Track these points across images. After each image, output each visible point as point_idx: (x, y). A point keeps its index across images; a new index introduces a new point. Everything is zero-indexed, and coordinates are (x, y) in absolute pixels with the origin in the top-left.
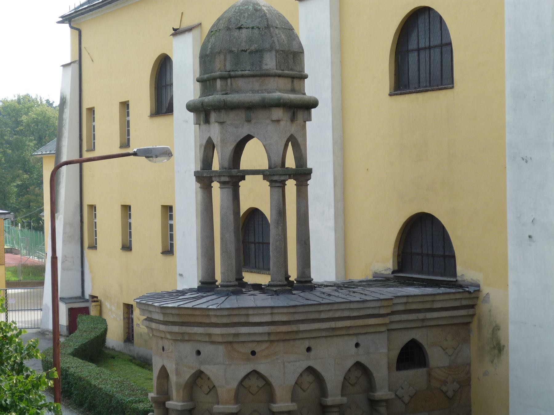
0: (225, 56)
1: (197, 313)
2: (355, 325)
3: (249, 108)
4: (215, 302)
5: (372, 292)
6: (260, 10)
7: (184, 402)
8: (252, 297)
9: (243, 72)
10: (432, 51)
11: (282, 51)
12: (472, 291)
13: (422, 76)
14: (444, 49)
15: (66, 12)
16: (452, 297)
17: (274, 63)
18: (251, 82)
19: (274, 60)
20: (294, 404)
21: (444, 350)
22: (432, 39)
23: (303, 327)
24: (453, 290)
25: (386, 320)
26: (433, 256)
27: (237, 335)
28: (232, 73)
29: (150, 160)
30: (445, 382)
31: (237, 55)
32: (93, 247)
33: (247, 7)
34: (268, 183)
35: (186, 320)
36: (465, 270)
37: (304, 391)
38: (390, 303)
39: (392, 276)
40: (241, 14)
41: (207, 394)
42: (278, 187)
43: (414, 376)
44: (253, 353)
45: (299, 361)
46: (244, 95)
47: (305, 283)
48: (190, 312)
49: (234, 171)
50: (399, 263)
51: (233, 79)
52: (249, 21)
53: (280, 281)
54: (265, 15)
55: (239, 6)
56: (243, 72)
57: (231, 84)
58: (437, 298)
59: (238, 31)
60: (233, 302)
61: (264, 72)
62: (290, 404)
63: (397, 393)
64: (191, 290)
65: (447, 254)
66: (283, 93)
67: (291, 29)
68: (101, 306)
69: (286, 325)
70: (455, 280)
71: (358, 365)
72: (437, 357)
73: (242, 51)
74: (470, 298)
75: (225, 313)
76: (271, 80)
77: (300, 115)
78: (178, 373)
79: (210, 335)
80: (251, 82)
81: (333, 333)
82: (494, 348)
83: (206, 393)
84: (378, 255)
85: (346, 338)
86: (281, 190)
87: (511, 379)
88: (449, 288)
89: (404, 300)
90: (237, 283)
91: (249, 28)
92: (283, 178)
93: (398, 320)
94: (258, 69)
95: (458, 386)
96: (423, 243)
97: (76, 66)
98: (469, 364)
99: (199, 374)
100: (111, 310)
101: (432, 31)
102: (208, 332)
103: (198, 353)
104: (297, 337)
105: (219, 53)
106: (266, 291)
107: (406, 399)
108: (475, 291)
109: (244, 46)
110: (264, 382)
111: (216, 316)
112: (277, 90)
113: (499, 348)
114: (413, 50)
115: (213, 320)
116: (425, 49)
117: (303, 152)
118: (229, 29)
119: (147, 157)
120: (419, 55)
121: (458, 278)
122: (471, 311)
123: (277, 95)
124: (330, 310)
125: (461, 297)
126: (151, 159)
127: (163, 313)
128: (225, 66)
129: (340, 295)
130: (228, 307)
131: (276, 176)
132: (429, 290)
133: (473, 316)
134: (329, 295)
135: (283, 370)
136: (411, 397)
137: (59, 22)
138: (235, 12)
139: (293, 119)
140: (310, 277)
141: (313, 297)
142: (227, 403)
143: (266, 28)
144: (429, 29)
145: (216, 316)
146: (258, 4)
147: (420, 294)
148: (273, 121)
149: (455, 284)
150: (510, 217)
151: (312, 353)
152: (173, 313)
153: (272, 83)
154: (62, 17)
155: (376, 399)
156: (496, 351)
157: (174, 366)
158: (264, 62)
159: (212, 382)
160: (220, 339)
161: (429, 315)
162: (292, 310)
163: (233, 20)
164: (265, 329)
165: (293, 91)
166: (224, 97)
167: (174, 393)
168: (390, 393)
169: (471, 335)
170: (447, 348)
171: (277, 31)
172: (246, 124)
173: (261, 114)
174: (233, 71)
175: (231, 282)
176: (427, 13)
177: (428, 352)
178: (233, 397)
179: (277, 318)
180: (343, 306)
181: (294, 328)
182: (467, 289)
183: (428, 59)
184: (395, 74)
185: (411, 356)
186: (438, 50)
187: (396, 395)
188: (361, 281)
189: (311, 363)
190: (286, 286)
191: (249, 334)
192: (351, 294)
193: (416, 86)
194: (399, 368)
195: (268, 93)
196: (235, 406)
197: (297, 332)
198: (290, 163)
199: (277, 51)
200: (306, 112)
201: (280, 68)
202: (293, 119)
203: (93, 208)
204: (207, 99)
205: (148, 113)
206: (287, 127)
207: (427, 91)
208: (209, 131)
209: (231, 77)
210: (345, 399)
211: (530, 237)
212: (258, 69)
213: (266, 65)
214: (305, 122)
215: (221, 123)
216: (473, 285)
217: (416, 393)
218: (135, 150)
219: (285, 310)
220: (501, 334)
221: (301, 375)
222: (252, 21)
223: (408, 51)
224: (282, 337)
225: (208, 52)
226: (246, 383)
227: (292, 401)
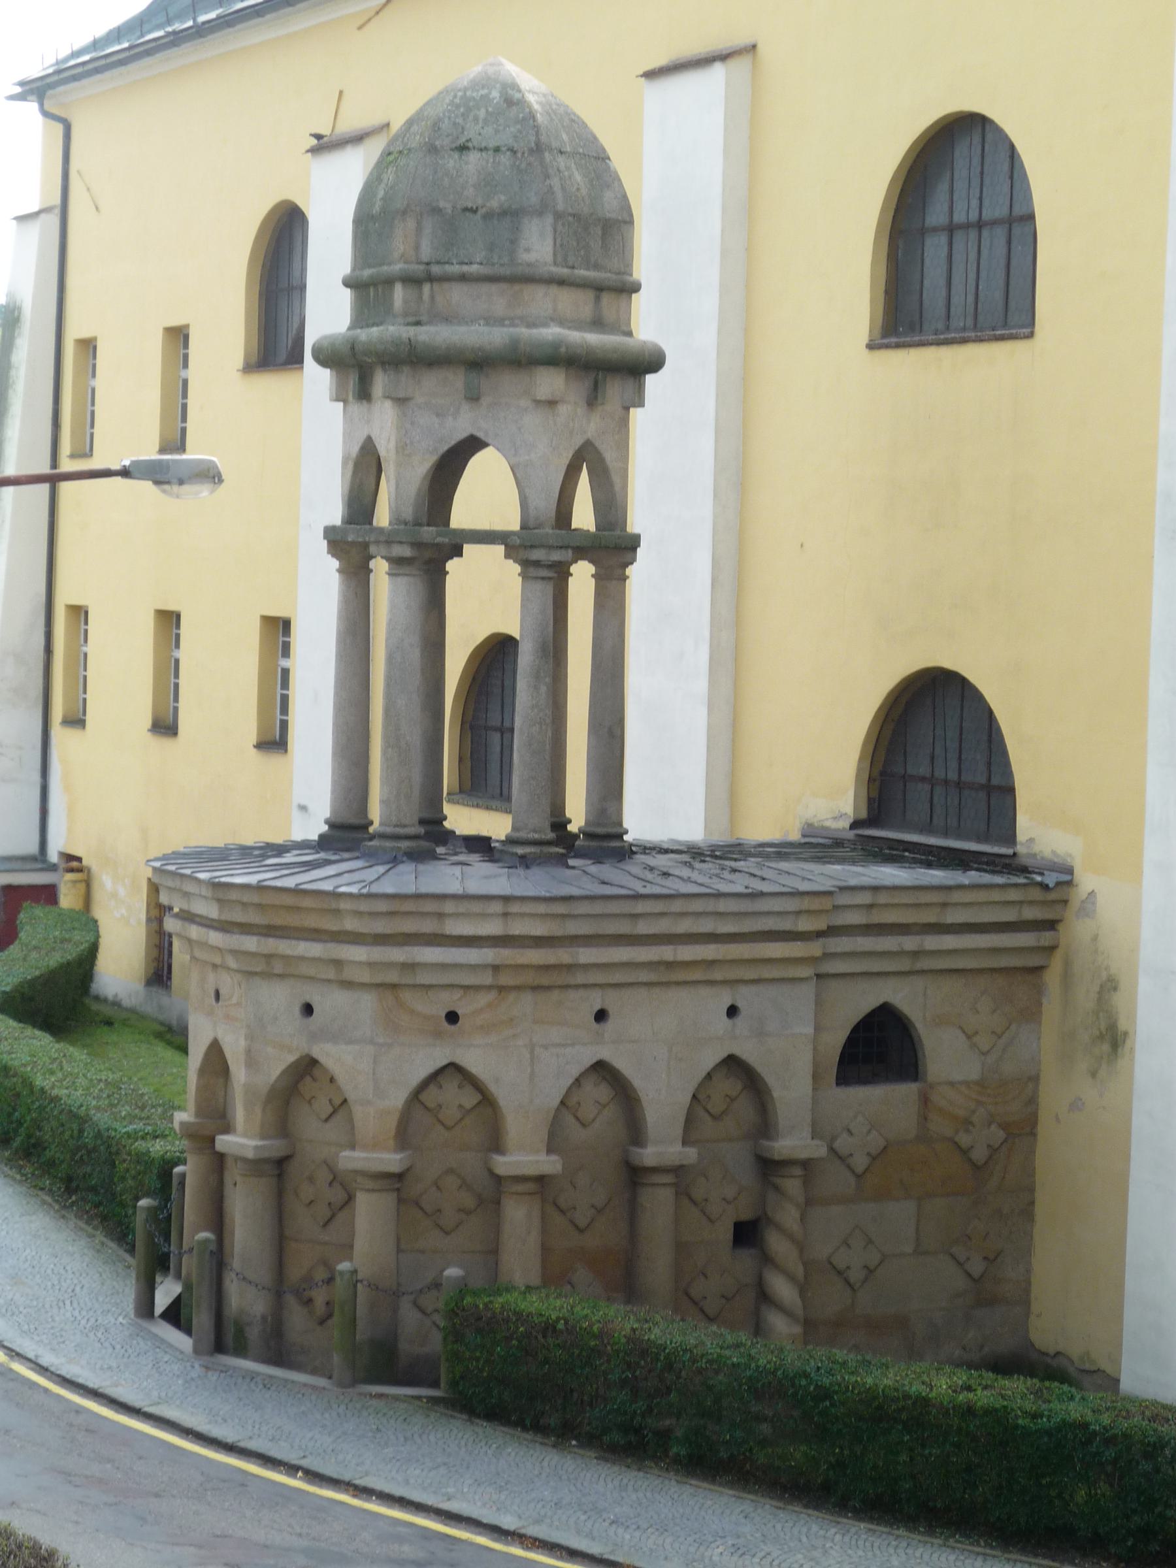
1: (307, 903)
2: (729, 957)
3: (478, 363)
4: (356, 876)
5: (781, 872)
6: (521, 103)
7: (263, 1138)
8: (457, 870)
9: (465, 268)
10: (985, 233)
11: (574, 216)
12: (1051, 885)
13: (956, 300)
14: (1017, 230)
15: (35, 70)
16: (996, 896)
18: (484, 295)
19: (549, 241)
20: (554, 1158)
21: (969, 1037)
22: (986, 203)
23: (586, 955)
24: (999, 880)
25: (814, 949)
26: (960, 785)
27: (410, 967)
28: (436, 270)
29: (164, 491)
30: (967, 1123)
31: (452, 221)
32: (76, 721)
33: (486, 91)
34: (517, 568)
35: (278, 921)
36: (1038, 830)
37: (584, 1125)
38: (827, 903)
39: (851, 835)
41: (326, 1120)
42: (543, 578)
43: (883, 1103)
44: (452, 1017)
45: (573, 1045)
47: (606, 841)
48: (289, 900)
49: (428, 533)
50: (870, 800)
51: (436, 286)
52: (489, 130)
53: (535, 831)
54: (532, 116)
55: (465, 90)
56: (465, 268)
57: (432, 297)
58: (957, 897)
59: (456, 155)
60: (405, 879)
62: (543, 1157)
63: (836, 1145)
64: (304, 845)
65: (995, 781)
66: (569, 328)
67: (602, 157)
68: (88, 884)
70: (1010, 851)
71: (732, 1063)
72: (947, 1055)
73: (466, 209)
74: (1044, 903)
75: (382, 906)
77: (615, 389)
78: (251, 1061)
79: (338, 963)
80: (484, 295)
81: (669, 977)
82: (1101, 1037)
83: (324, 1117)
84: (815, 777)
85: (704, 991)
86: (549, 588)
87: (1139, 1122)
88: (993, 872)
89: (864, 898)
90: (421, 830)
91: (486, 149)
92: (556, 556)
94: (506, 260)
95: (1002, 1134)
96: (935, 751)
97: (54, 220)
98: (1035, 1079)
99: (307, 1067)
100: (114, 895)
101: (987, 181)
102: (334, 956)
103: (308, 1009)
104: (571, 980)
105: (404, 212)
106: (497, 856)
107: (860, 1162)
108: (1058, 884)
109: (471, 197)
110: (479, 1097)
111: (359, 914)
112: (555, 321)
113: (1113, 1040)
114: (935, 230)
115: (350, 924)
116: (967, 226)
117: (617, 488)
118: (432, 149)
119: (157, 483)
120: (950, 244)
121: (1020, 849)
122: (1046, 938)
123: (551, 332)
124: (663, 914)
125: (1022, 899)
126: (166, 487)
127: (219, 901)
128: (417, 248)
129: (695, 876)
130: (390, 890)
131: (543, 549)
132: (937, 876)
133: (1052, 949)
134: (666, 874)
135: (528, 1066)
136: (874, 1159)
137: (12, 98)
138: (452, 103)
139: (593, 400)
140: (620, 824)
141: (622, 878)
142: (375, 1146)
143: (531, 151)
144: (982, 173)
145: (359, 914)
146: (515, 87)
147: (909, 883)
148: (538, 402)
149: (1010, 865)
151: (610, 1026)
152: (245, 900)
153: (541, 300)
154: (22, 84)
155: (776, 1157)
156: (1106, 1047)
157: (243, 1042)
159: (339, 1088)
160: (365, 977)
161: (932, 942)
162: (560, 909)
163: (445, 125)
164: (487, 955)
165: (598, 324)
167: (239, 1115)
168: (816, 1142)
169: (1044, 1001)
170: (976, 1033)
171: (561, 161)
172: (465, 407)
173: (508, 382)
174: (438, 263)
175: (405, 826)
177: (925, 1041)
178: (393, 1133)
179: (518, 928)
180: (698, 906)
181: (563, 956)
182: (1039, 878)
183: (973, 256)
184: (886, 292)
185: (879, 1048)
186: (1000, 233)
187: (832, 1150)
188: (762, 845)
189: (604, 1053)
190: (557, 843)
191: (444, 967)
192: (726, 875)
193: (941, 326)
194: (843, 1079)
195: (530, 325)
196: (398, 1156)
197: (570, 968)
198: (584, 517)
199: (558, 216)
200: (630, 383)
201: (565, 259)
202: (593, 400)
203: (79, 613)
205: (239, 361)
206: (577, 422)
207: (964, 341)
209: (431, 279)
210: (691, 1155)
212: (506, 260)
213: (528, 250)
214: (627, 409)
215: (401, 402)
217: (885, 1148)
218: (127, 463)
219: (542, 908)
220: (1119, 1000)
221: (577, 1082)
223: (923, 232)
224: (529, 978)
225: (377, 209)
226: (431, 1096)
227: (549, 1151)
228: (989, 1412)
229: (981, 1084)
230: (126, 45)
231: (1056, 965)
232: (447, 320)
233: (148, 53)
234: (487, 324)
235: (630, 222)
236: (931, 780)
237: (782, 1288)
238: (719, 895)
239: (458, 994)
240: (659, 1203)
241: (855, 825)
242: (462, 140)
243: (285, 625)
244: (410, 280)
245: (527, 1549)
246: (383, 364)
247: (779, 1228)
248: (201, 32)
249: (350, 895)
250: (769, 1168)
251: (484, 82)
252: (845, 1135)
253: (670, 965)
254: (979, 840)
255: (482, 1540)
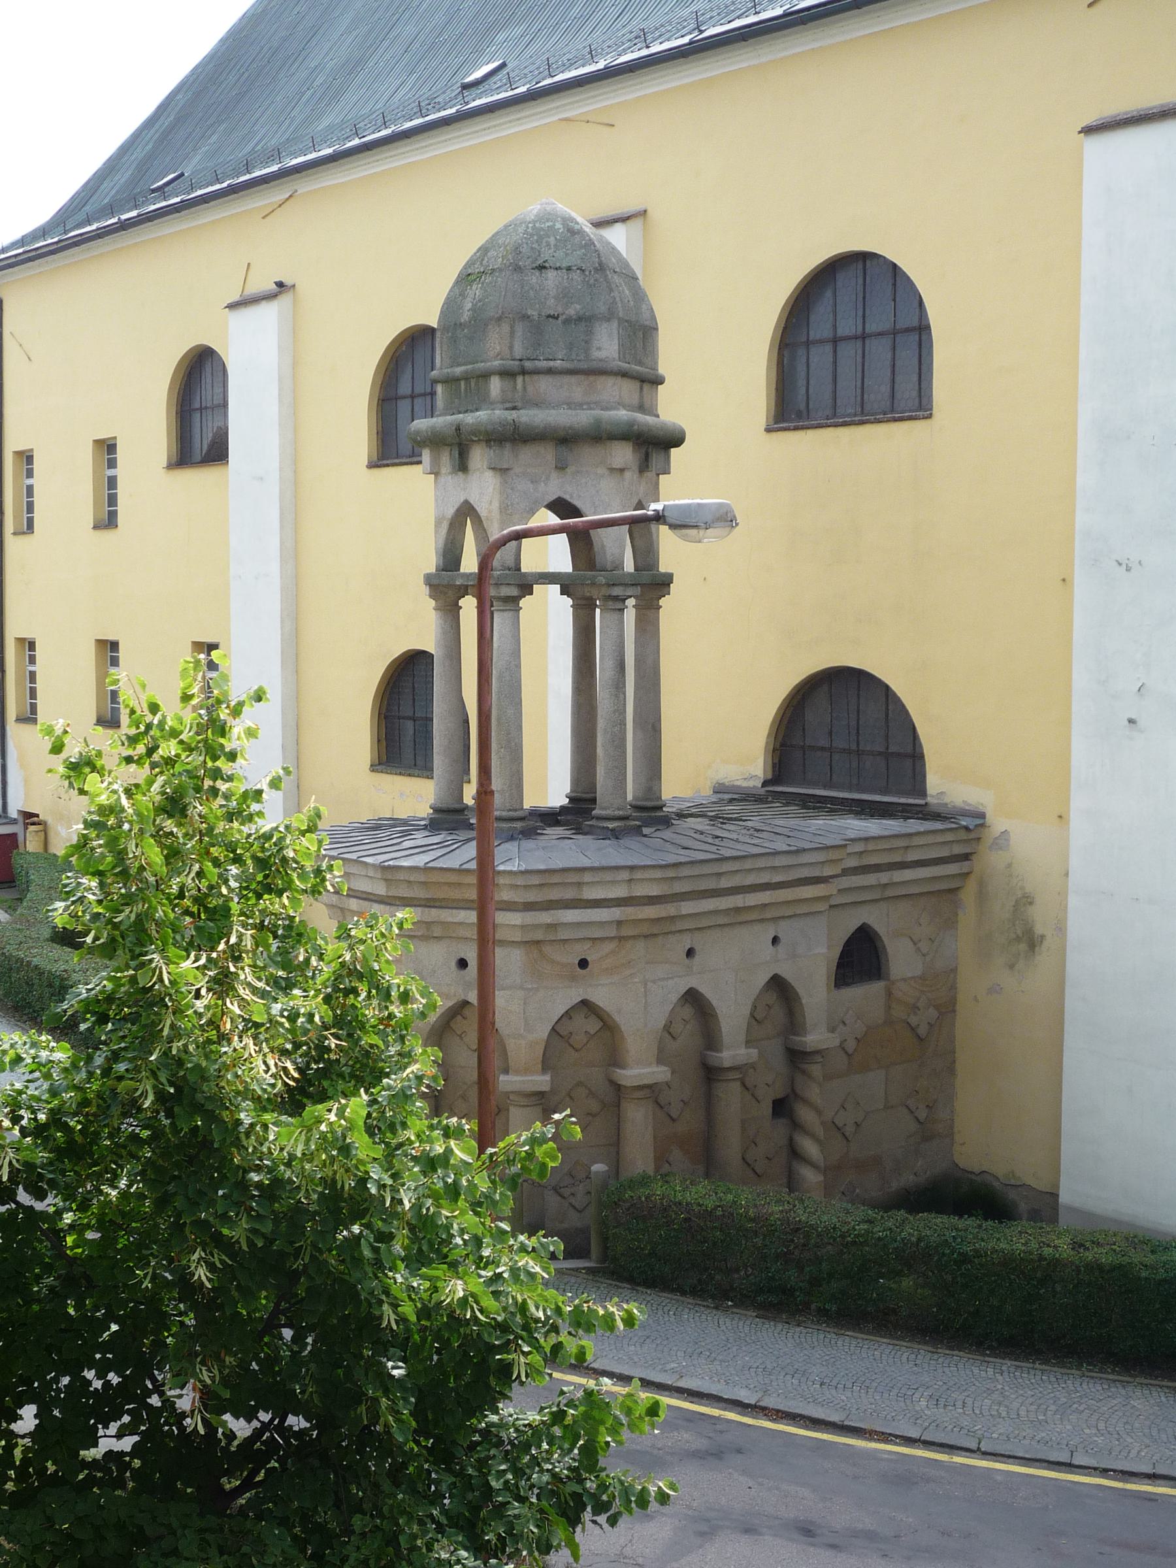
0: (512, 327)
9: (551, 363)
17: (616, 347)
19: (616, 341)
21: (915, 944)
23: (688, 907)
28: (528, 365)
30: (915, 1008)
31: (537, 327)
35: (440, 894)
36: (943, 783)
39: (762, 791)
40: (541, 238)
44: (583, 964)
46: (553, 412)
47: (650, 814)
48: (453, 878)
50: (774, 765)
51: (527, 378)
53: (619, 809)
55: (534, 222)
56: (551, 363)
57: (525, 388)
59: (537, 273)
61: (594, 365)
62: (655, 1069)
68: (45, 832)
69: (653, 904)
70: (922, 802)
71: (778, 984)
72: (902, 960)
73: (549, 316)
75: (536, 880)
76: (610, 381)
81: (737, 918)
82: (1018, 939)
85: (757, 927)
89: (859, 847)
93: (846, 886)
95: (935, 1014)
98: (954, 970)
105: (499, 319)
107: (851, 1045)
112: (614, 404)
118: (518, 269)
122: (964, 867)
123: (623, 414)
127: (386, 880)
128: (511, 347)
135: (639, 1000)
138: (525, 232)
142: (527, 1071)
143: (596, 270)
144: (864, 298)
146: (573, 220)
149: (925, 813)
150: (1080, 679)
151: (697, 959)
152: (412, 879)
156: (1023, 947)
158: (596, 344)
162: (671, 873)
164: (615, 913)
165: (641, 408)
166: (514, 415)
169: (960, 913)
171: (616, 279)
172: (554, 475)
173: (588, 454)
174: (529, 359)
176: (860, 266)
177: (889, 950)
179: (640, 891)
181: (669, 910)
184: (777, 389)
185: (860, 958)
189: (693, 982)
191: (579, 924)
193: (829, 412)
196: (547, 1078)
197: (672, 919)
200: (662, 454)
204: (469, 419)
205: (164, 461)
208: (465, 489)
209: (524, 372)
211: (1131, 721)
213: (599, 349)
215: (501, 471)
216: (965, 813)
219: (658, 874)
222: (567, 255)
223: (808, 344)
224: (645, 929)
225: (465, 316)
227: (660, 1061)
228: (1114, 1268)
229: (923, 978)
230: (56, 240)
231: (971, 887)
232: (537, 405)
233: (76, 244)
234: (570, 408)
235: (657, 329)
236: (830, 750)
237: (810, 1148)
238: (776, 853)
239: (588, 945)
240: (730, 1097)
241: (765, 784)
242: (540, 262)
243: (114, 646)
244: (507, 374)
245: (773, 1421)
246: (488, 441)
247: (805, 1101)
248: (124, 226)
249: (510, 872)
250: (796, 1057)
251: (547, 216)
252: (841, 1026)
253: (737, 910)
254: (825, 787)
255: (731, 1416)
